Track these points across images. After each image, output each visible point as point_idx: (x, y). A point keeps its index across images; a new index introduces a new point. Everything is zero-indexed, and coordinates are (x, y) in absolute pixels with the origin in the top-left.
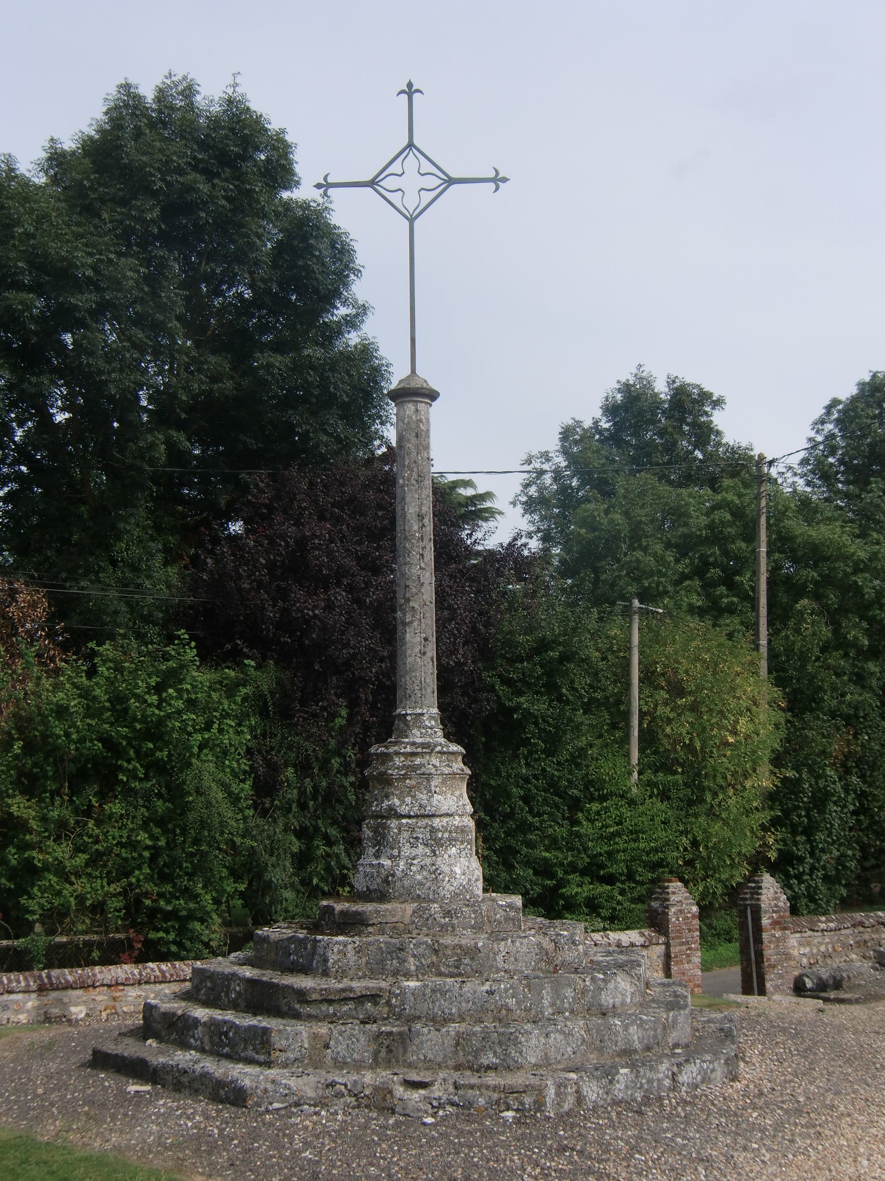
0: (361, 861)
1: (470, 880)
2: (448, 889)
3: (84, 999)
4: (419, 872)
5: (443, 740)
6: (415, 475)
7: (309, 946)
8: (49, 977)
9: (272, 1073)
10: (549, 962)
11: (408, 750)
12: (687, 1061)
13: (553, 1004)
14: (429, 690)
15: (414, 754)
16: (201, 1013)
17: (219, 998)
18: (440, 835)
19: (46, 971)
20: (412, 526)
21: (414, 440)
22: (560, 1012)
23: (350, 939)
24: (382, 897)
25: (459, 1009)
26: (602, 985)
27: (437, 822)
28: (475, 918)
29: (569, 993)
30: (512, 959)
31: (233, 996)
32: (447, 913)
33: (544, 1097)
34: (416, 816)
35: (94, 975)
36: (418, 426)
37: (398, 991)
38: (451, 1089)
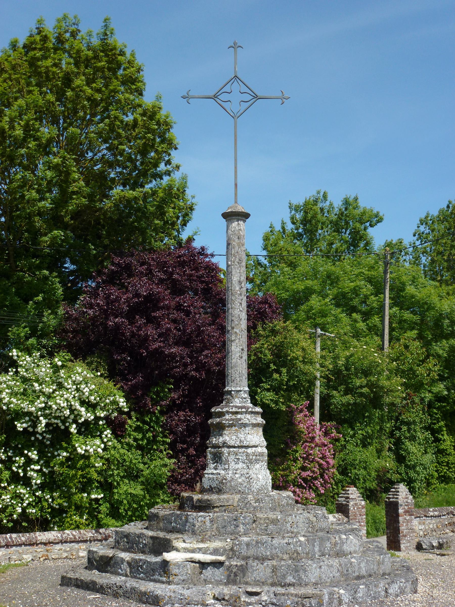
0: (206, 472)
1: (266, 482)
2: (255, 487)
3: (31, 551)
4: (240, 478)
5: (251, 405)
6: (237, 260)
7: (183, 518)
8: (11, 537)
9: (172, 587)
10: (313, 527)
11: (234, 410)
12: (393, 582)
13: (320, 551)
14: (244, 377)
15: (237, 413)
16: (126, 556)
17: (132, 547)
18: (251, 457)
19: (9, 535)
20: (235, 287)
21: (237, 240)
22: (323, 555)
23: (207, 514)
24: (219, 491)
25: (271, 553)
26: (344, 541)
27: (250, 450)
28: (272, 503)
29: (328, 545)
30: (295, 526)
31: (141, 546)
32: (257, 501)
33: (323, 600)
34: (239, 447)
35: (36, 537)
36: (239, 233)
37: (237, 543)
38: (272, 596)
